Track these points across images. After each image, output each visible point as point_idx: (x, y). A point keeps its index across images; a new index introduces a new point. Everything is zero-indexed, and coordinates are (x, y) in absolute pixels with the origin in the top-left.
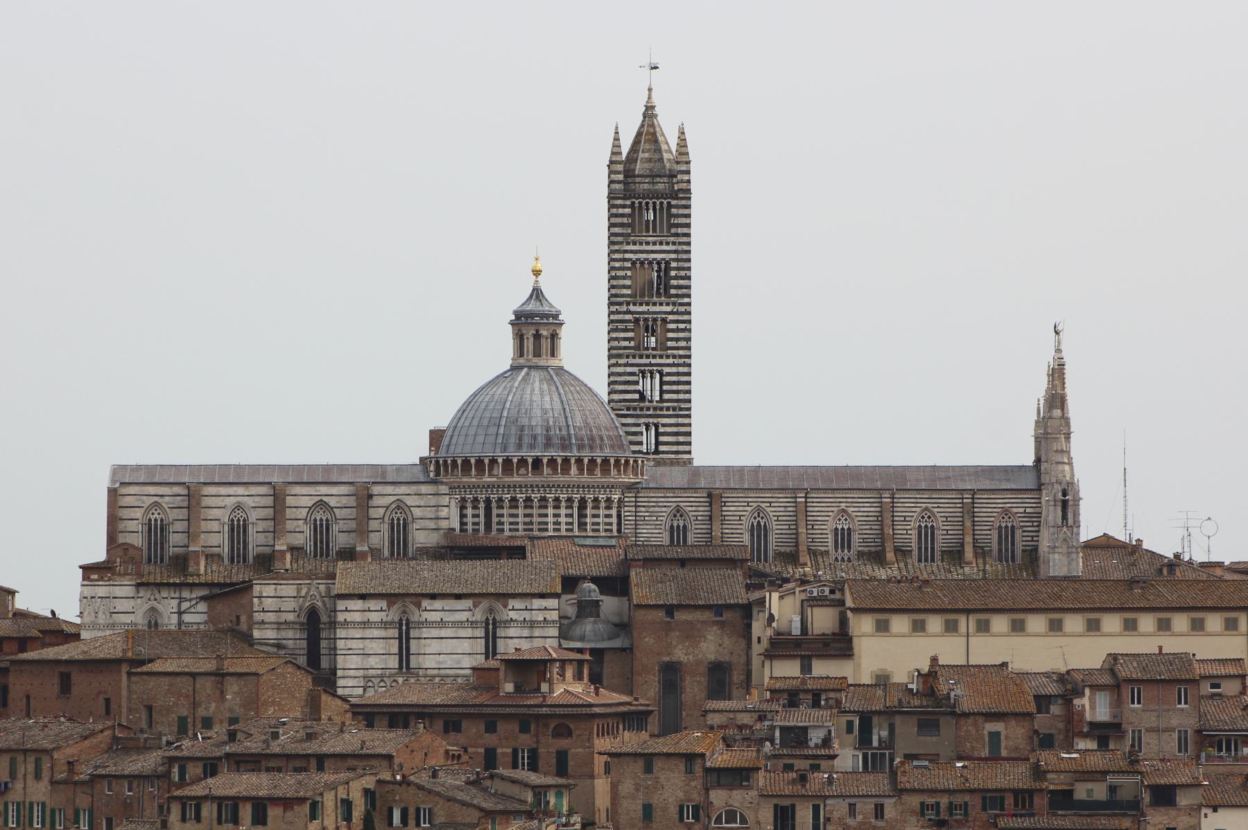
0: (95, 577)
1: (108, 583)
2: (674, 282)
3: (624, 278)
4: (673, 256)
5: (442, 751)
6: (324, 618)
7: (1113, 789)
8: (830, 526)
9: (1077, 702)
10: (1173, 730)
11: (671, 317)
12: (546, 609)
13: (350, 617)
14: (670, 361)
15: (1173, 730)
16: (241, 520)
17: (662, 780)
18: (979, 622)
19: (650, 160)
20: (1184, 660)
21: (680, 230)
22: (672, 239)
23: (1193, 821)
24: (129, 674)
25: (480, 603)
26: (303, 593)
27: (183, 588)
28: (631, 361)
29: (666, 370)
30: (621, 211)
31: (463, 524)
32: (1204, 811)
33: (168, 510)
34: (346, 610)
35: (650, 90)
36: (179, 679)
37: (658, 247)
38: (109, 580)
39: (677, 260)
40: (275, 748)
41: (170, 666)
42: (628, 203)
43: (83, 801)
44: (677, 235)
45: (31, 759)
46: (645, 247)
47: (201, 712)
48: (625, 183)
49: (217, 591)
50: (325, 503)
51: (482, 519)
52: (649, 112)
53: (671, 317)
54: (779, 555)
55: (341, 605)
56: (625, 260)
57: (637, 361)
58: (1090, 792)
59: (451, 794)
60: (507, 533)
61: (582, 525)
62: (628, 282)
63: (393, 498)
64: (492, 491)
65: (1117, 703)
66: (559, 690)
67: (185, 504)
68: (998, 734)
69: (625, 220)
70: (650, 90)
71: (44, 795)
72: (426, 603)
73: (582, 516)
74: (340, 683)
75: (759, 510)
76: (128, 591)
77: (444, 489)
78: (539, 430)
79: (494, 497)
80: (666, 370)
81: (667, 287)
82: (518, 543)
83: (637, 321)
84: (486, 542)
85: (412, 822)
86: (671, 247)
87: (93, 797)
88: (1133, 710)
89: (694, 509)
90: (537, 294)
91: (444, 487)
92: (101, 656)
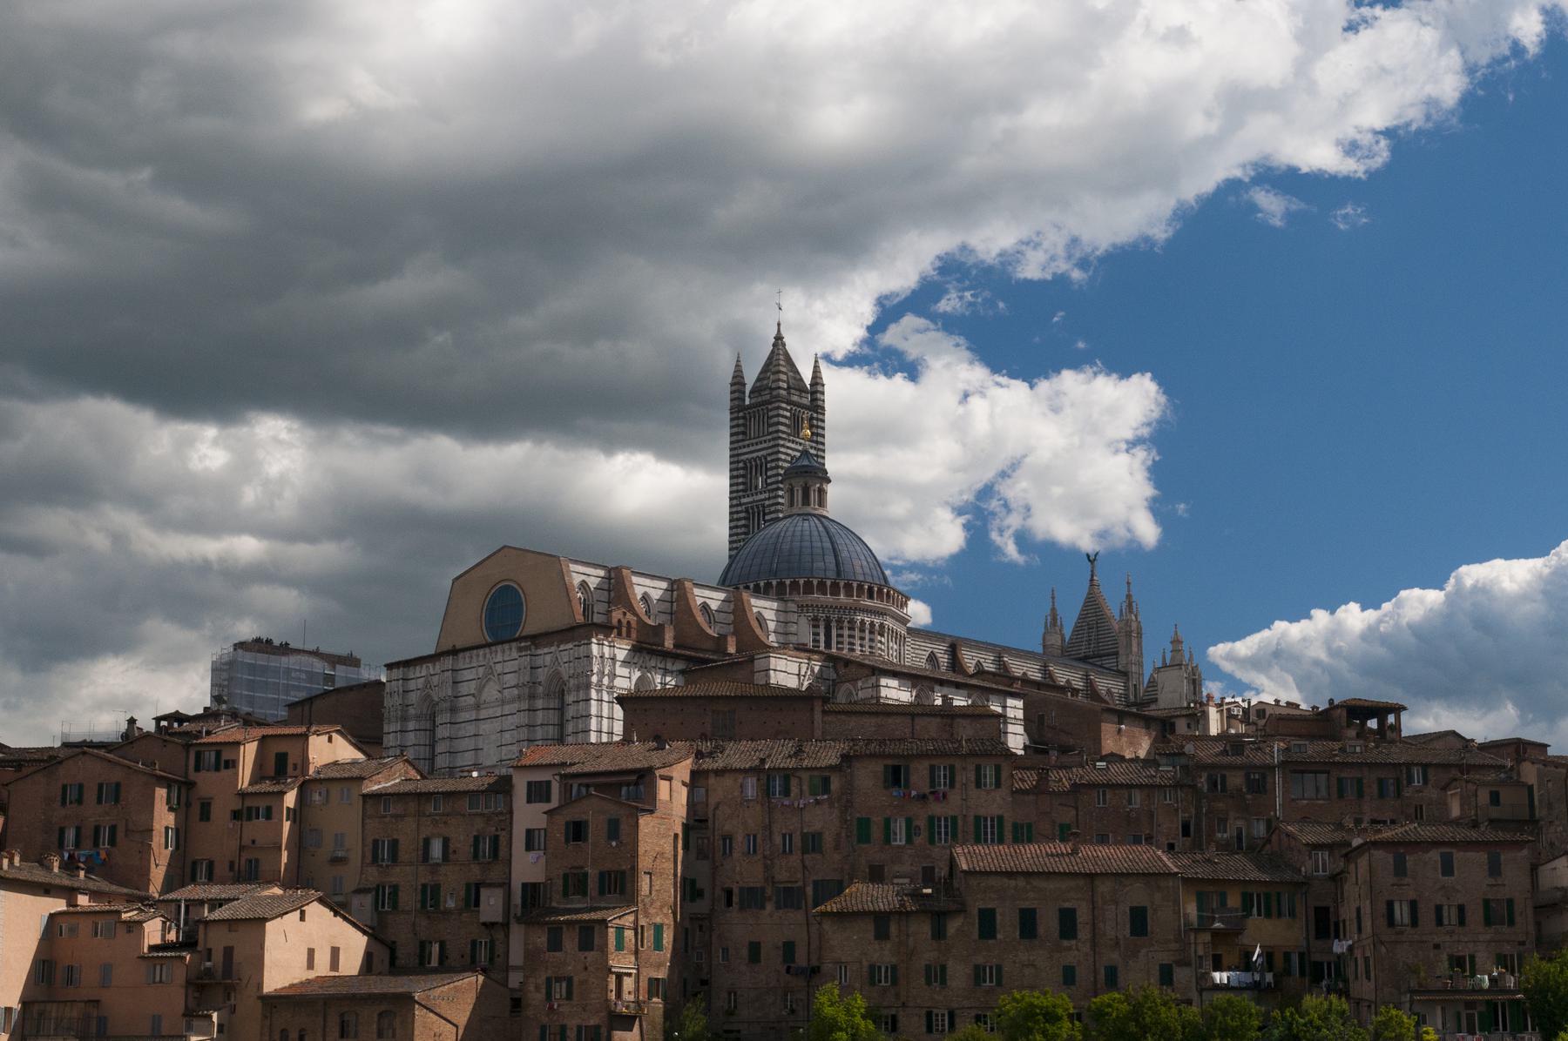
12: (1015, 708)
21: (820, 439)
24: (824, 712)
26: (803, 673)
27: (668, 660)
34: (886, 687)
35: (779, 325)
36: (890, 720)
42: (789, 408)
44: (817, 442)
50: (708, 605)
52: (779, 338)
67: (606, 587)
69: (787, 422)
70: (779, 325)
77: (792, 606)
87: (1077, 809)
91: (793, 605)
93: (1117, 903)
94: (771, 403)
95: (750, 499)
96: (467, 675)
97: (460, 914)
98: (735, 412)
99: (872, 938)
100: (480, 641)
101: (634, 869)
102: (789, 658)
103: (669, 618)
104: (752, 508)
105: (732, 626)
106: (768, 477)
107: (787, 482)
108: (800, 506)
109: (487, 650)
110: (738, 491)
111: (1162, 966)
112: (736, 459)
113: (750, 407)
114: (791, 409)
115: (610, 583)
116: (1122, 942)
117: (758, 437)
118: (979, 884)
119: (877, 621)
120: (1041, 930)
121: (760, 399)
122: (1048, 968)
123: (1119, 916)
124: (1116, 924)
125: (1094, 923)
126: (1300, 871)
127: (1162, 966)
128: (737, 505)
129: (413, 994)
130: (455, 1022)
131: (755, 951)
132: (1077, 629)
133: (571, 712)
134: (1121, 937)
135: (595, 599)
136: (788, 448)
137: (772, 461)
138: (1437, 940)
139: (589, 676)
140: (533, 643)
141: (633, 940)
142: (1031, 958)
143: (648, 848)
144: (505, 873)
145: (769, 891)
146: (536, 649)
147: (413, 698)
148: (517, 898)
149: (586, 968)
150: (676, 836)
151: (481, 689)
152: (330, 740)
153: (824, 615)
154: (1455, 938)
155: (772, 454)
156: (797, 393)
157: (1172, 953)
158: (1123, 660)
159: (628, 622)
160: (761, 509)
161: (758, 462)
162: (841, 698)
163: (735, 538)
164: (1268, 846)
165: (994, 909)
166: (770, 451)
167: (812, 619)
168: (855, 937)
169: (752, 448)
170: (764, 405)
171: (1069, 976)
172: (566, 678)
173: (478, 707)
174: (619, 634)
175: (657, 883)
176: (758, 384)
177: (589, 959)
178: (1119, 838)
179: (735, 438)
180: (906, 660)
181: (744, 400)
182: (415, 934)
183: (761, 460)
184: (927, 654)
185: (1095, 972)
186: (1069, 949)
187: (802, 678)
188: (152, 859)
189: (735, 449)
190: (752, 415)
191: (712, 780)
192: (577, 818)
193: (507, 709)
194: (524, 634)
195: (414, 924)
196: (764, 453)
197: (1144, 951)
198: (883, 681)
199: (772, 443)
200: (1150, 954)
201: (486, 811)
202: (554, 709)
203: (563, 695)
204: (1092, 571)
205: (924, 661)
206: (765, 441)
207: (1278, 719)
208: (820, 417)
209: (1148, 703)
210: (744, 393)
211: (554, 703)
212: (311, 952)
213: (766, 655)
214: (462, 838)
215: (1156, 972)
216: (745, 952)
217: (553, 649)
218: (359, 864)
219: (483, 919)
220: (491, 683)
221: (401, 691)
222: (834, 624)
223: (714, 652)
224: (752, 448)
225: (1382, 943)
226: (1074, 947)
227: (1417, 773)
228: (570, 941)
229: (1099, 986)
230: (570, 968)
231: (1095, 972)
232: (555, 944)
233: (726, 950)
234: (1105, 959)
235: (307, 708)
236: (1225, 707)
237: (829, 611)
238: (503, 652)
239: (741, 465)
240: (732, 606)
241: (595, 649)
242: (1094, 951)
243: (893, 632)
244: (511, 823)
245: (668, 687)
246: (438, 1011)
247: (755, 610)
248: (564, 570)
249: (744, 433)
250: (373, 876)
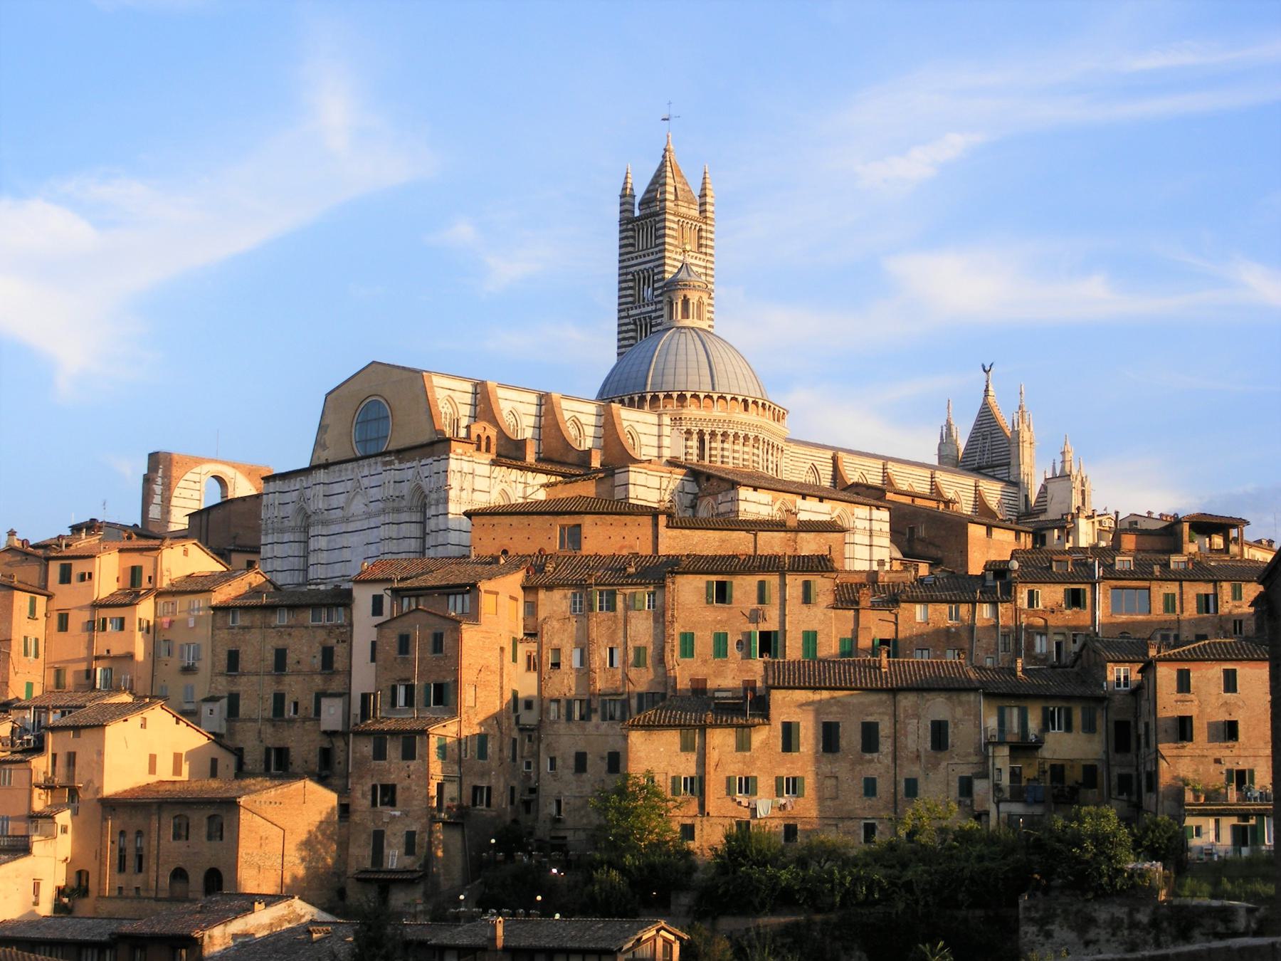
0: (459, 451)
1: (471, 459)
4: (704, 271)
12: (881, 520)
16: (512, 424)
21: (709, 251)
22: (703, 257)
25: (836, 508)
26: (664, 486)
33: (458, 405)
34: (746, 500)
38: (471, 456)
39: (706, 275)
42: (676, 219)
44: (706, 254)
49: (553, 479)
56: (674, 266)
63: (629, 423)
64: (718, 425)
71: (821, 622)
72: (799, 500)
76: (485, 470)
86: (704, 264)
89: (822, 467)
93: (918, 717)
94: (660, 214)
95: (638, 311)
96: (337, 488)
97: (304, 722)
98: (624, 224)
99: (679, 750)
100: (350, 455)
101: (456, 681)
102: (649, 472)
103: (538, 432)
104: (645, 318)
105: (602, 439)
106: (654, 290)
107: (666, 295)
108: (679, 317)
109: (355, 464)
110: (626, 303)
111: (961, 779)
112: (625, 271)
113: (639, 219)
114: (679, 221)
115: (476, 399)
116: (923, 755)
117: (647, 249)
118: (784, 698)
119: (751, 435)
120: (843, 743)
121: (648, 211)
122: (849, 780)
123: (920, 730)
124: (917, 737)
125: (895, 736)
126: (1102, 685)
127: (961, 779)
128: (625, 317)
129: (238, 800)
130: (282, 826)
131: (581, 762)
132: (972, 441)
133: (432, 524)
134: (921, 750)
135: (460, 415)
136: (675, 259)
137: (659, 273)
138: (1218, 755)
139: (447, 491)
140: (397, 458)
141: (456, 750)
142: (834, 771)
143: (472, 661)
144: (345, 684)
145: (594, 704)
146: (400, 463)
147: (289, 509)
148: (356, 708)
149: (409, 777)
150: (502, 649)
151: (349, 501)
152: (186, 553)
153: (697, 428)
154: (1235, 751)
155: (657, 266)
156: (686, 205)
157: (971, 766)
158: (1013, 471)
159: (488, 438)
160: (648, 320)
161: (646, 274)
162: (703, 512)
163: (623, 350)
164: (1079, 662)
165: (798, 724)
166: (657, 263)
167: (685, 433)
168: (662, 749)
169: (640, 260)
170: (651, 217)
171: (870, 787)
172: (427, 492)
173: (347, 520)
174: (479, 449)
175: (482, 694)
176: (648, 196)
177: (412, 768)
178: (938, 653)
179: (624, 250)
180: (784, 472)
181: (633, 212)
182: (262, 741)
183: (648, 272)
184: (808, 466)
185: (896, 784)
186: (871, 761)
187: (663, 492)
188: (11, 667)
189: (624, 261)
190: (640, 226)
191: (542, 595)
192: (405, 631)
193: (373, 522)
194: (389, 449)
195: (260, 732)
196: (651, 265)
197: (944, 764)
198: (744, 493)
199: (659, 255)
200: (950, 768)
201: (328, 623)
202: (416, 522)
203: (425, 509)
204: (987, 381)
205: (805, 473)
206: (652, 253)
207: (939, 547)
208: (709, 228)
209: (1038, 513)
210: (633, 205)
211: (416, 517)
212: (153, 758)
213: (626, 469)
214: (305, 649)
215: (955, 785)
216: (572, 762)
217: (414, 464)
218: (209, 675)
219: (323, 728)
220: (359, 497)
221: (277, 503)
222: (707, 437)
223: (579, 466)
224: (640, 260)
225: (1163, 758)
226: (876, 760)
227: (1226, 587)
228: (393, 750)
229: (899, 797)
230: (393, 777)
231: (896, 784)
232: (380, 754)
233: (553, 760)
234: (905, 771)
235: (204, 517)
236: (1097, 519)
237: (702, 424)
238: (370, 465)
239: (630, 277)
240: (602, 419)
241: (453, 464)
242: (896, 764)
243: (768, 444)
244: (351, 636)
245: (528, 500)
246: (264, 815)
247: (625, 424)
248: (427, 386)
249: (633, 245)
250: (222, 686)
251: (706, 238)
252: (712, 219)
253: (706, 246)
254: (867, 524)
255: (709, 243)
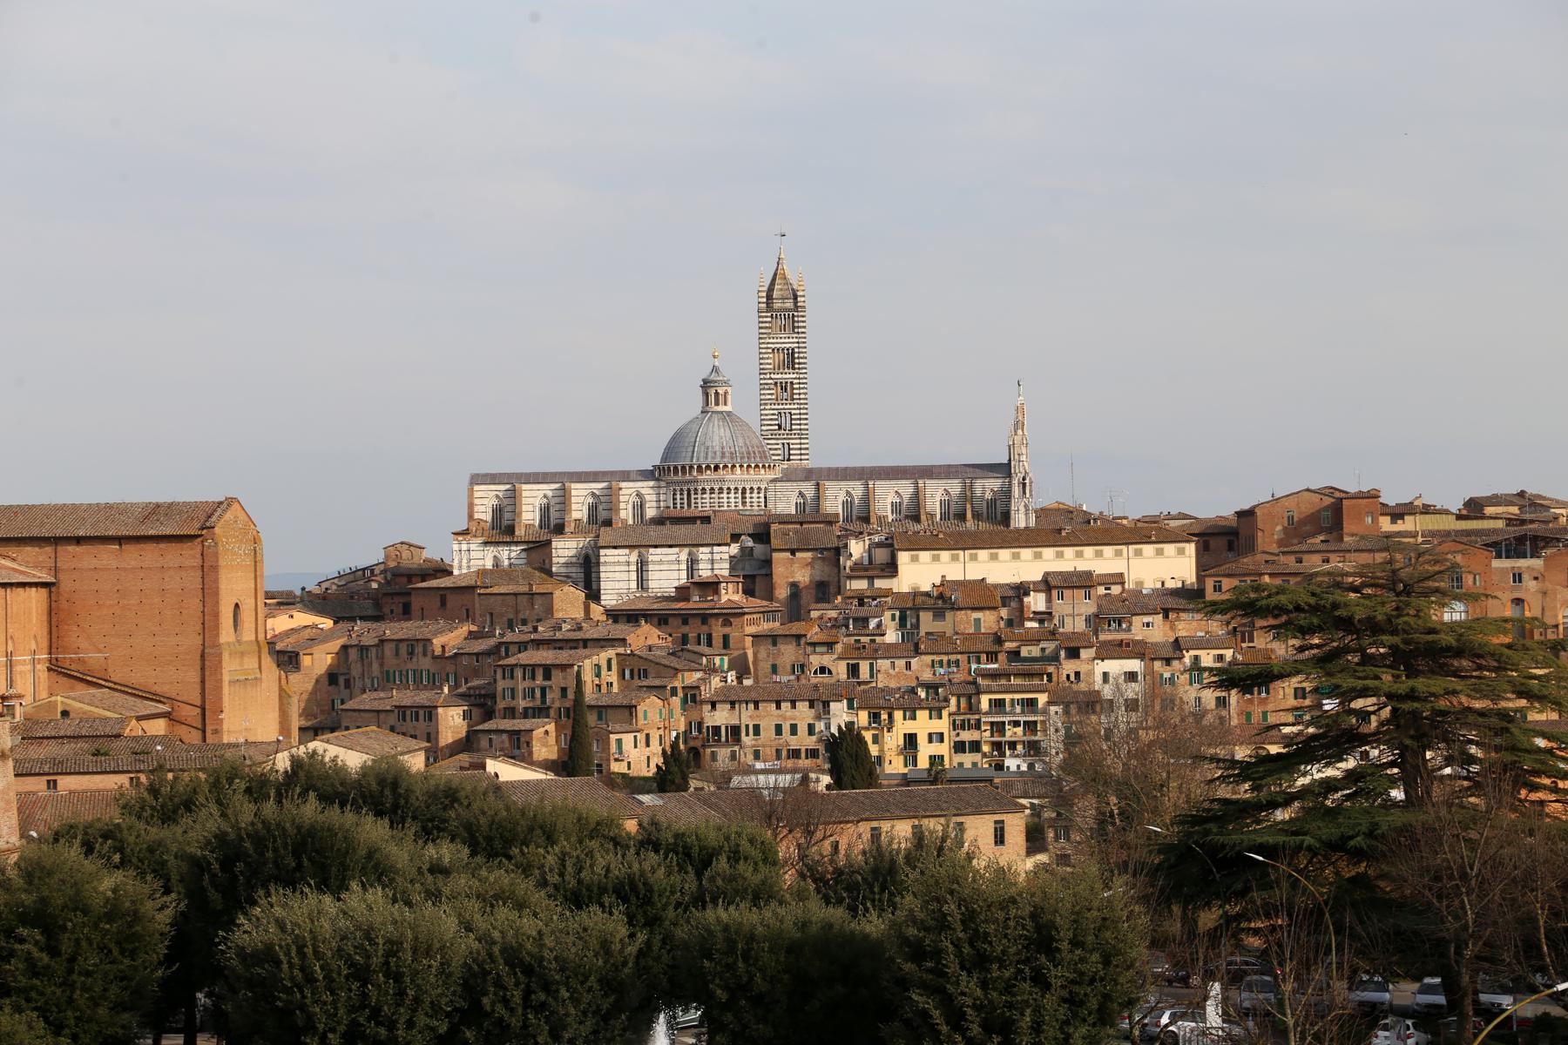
0: (460, 538)
2: (797, 361)
3: (768, 358)
5: (656, 636)
6: (593, 560)
7: (1043, 650)
8: (889, 501)
9: (1026, 600)
10: (1082, 615)
11: (795, 381)
13: (608, 559)
14: (796, 406)
15: (1082, 615)
17: (782, 650)
18: (971, 555)
19: (781, 290)
20: (1089, 574)
21: (800, 330)
23: (1090, 667)
28: (773, 407)
29: (793, 412)
30: (765, 319)
31: (675, 504)
32: (1096, 661)
37: (787, 340)
40: (559, 635)
41: (503, 590)
43: (450, 668)
45: (421, 644)
46: (779, 340)
47: (521, 616)
48: (767, 303)
51: (686, 501)
53: (795, 381)
54: (859, 518)
55: (602, 552)
56: (767, 348)
57: (776, 407)
58: (1030, 652)
59: (658, 661)
60: (700, 509)
61: (744, 503)
62: (769, 361)
65: (1049, 600)
66: (724, 599)
68: (979, 619)
69: (767, 325)
73: (744, 498)
74: (603, 597)
75: (848, 493)
77: (663, 484)
78: (717, 449)
79: (692, 488)
80: (793, 412)
81: (793, 363)
82: (706, 514)
83: (776, 383)
84: (688, 515)
85: (636, 677)
86: (796, 340)
88: (1058, 604)
90: (715, 369)
92: (463, 584)
251: (798, 322)
252: (804, 307)
253: (798, 327)
254: (710, 556)
255: (801, 324)
